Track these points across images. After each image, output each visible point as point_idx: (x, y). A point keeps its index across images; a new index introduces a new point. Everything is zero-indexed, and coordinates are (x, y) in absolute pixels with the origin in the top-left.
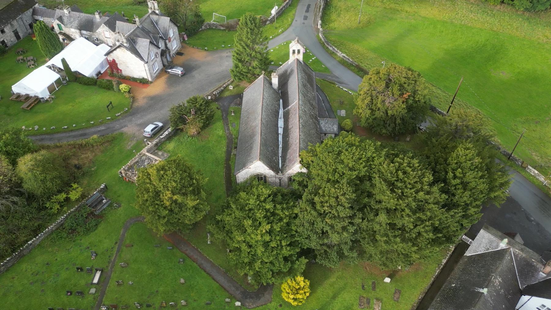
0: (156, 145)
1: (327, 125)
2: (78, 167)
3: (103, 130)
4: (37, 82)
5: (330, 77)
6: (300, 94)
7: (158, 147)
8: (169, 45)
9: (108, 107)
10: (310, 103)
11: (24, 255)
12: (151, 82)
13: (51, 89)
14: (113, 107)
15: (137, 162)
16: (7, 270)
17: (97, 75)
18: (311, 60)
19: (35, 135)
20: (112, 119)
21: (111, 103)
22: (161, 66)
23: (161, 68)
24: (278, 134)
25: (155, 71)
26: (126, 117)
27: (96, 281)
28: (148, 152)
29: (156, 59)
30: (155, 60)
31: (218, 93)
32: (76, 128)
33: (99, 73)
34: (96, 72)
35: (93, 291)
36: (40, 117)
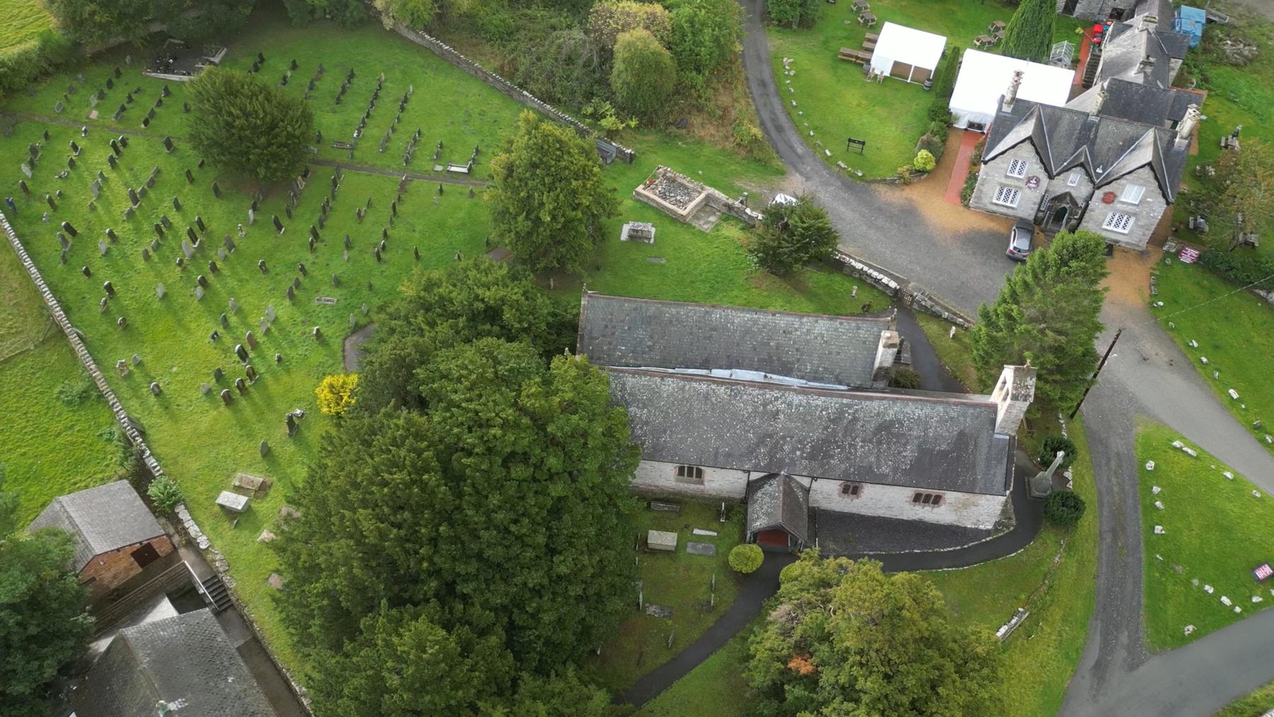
0: (730, 207)
1: (767, 499)
2: (681, 124)
3: (794, 151)
4: (906, 46)
5: (1124, 638)
6: (834, 403)
7: (730, 214)
8: (1096, 203)
9: (850, 140)
10: (826, 441)
11: (511, 96)
12: (967, 206)
13: (900, 69)
14: (861, 154)
15: (687, 188)
16: (493, 87)
17: (971, 125)
18: (1210, 589)
19: (774, 75)
20: (828, 158)
21: (863, 143)
22: (1028, 212)
23: (1021, 214)
24: (706, 365)
25: (1001, 202)
26: (839, 177)
27: (453, 169)
28: (708, 197)
29: (1021, 184)
30: (1017, 184)
31: (918, 302)
32: (796, 118)
33: (980, 127)
34: (977, 121)
35: (439, 168)
36: (821, 73)
